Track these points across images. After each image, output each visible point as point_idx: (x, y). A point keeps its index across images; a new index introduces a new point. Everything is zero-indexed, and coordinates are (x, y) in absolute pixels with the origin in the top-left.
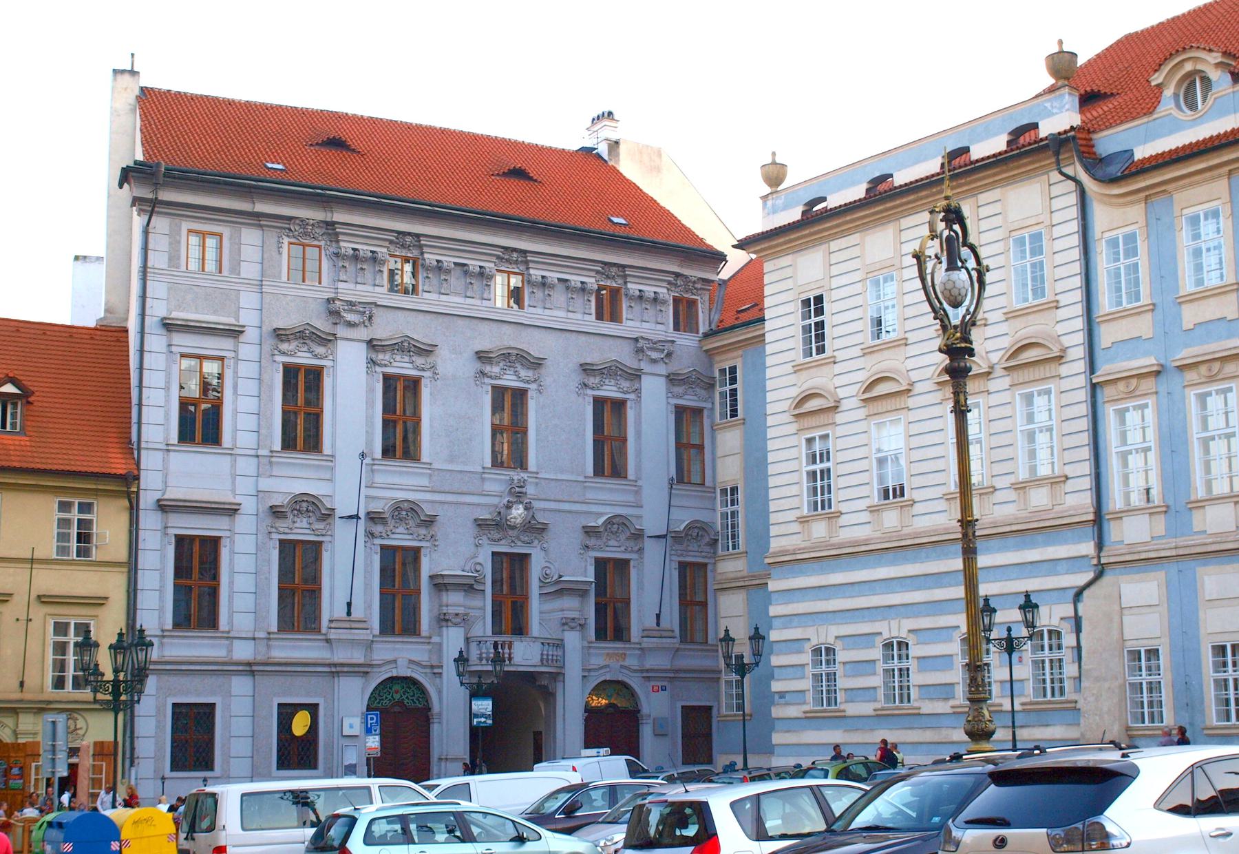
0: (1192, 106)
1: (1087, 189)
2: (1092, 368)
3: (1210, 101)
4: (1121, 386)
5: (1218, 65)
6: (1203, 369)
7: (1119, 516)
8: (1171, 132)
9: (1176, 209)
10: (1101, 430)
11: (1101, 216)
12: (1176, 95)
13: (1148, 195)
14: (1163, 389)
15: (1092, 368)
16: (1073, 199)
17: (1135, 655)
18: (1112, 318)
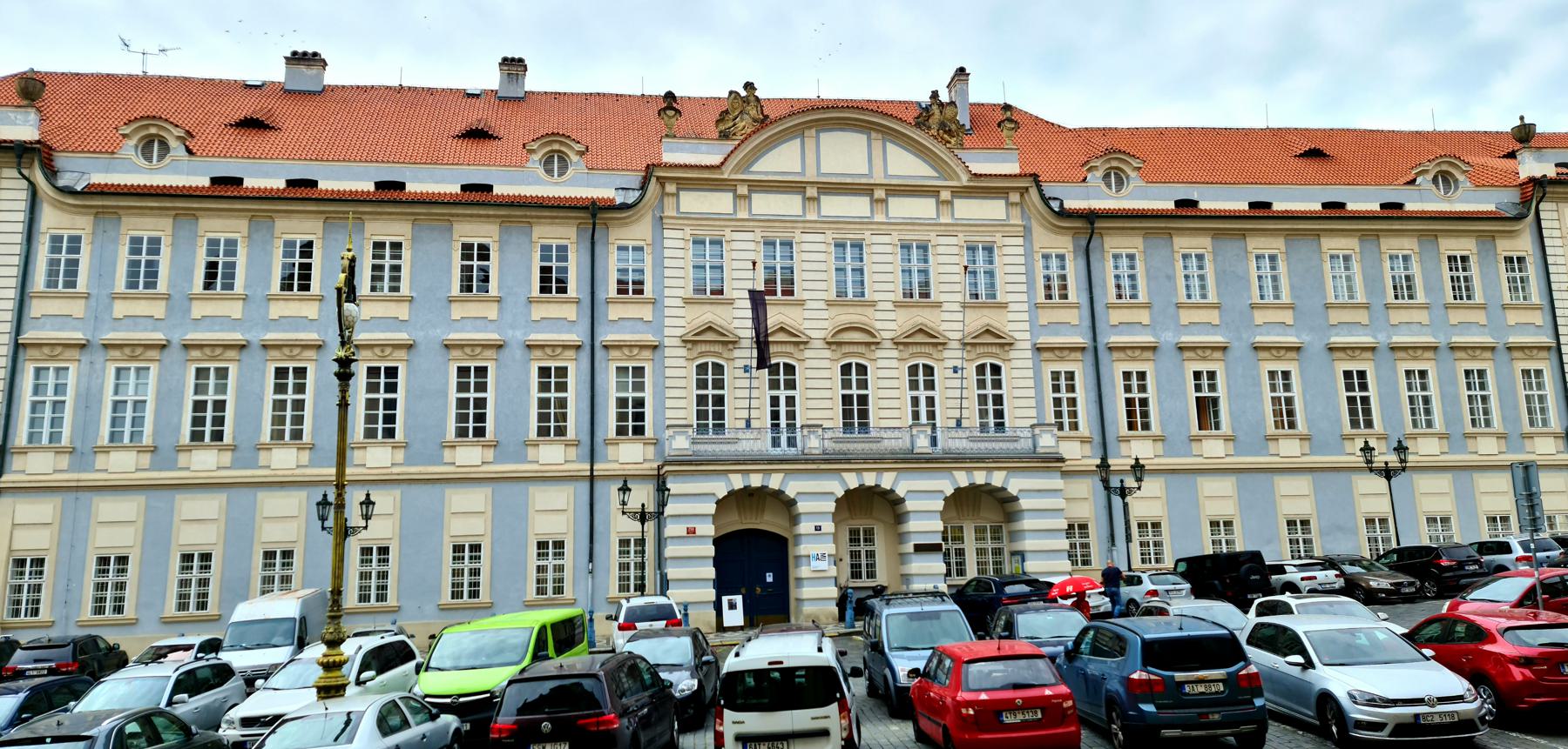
0: (149, 158)
1: (40, 193)
2: (18, 330)
3: (167, 160)
4: (46, 350)
5: (179, 138)
6: (127, 351)
7: (23, 451)
8: (128, 172)
9: (123, 230)
10: (17, 381)
11: (52, 220)
12: (136, 147)
13: (99, 213)
14: (83, 359)
15: (18, 330)
16: (24, 195)
17: (21, 563)
18: (42, 296)
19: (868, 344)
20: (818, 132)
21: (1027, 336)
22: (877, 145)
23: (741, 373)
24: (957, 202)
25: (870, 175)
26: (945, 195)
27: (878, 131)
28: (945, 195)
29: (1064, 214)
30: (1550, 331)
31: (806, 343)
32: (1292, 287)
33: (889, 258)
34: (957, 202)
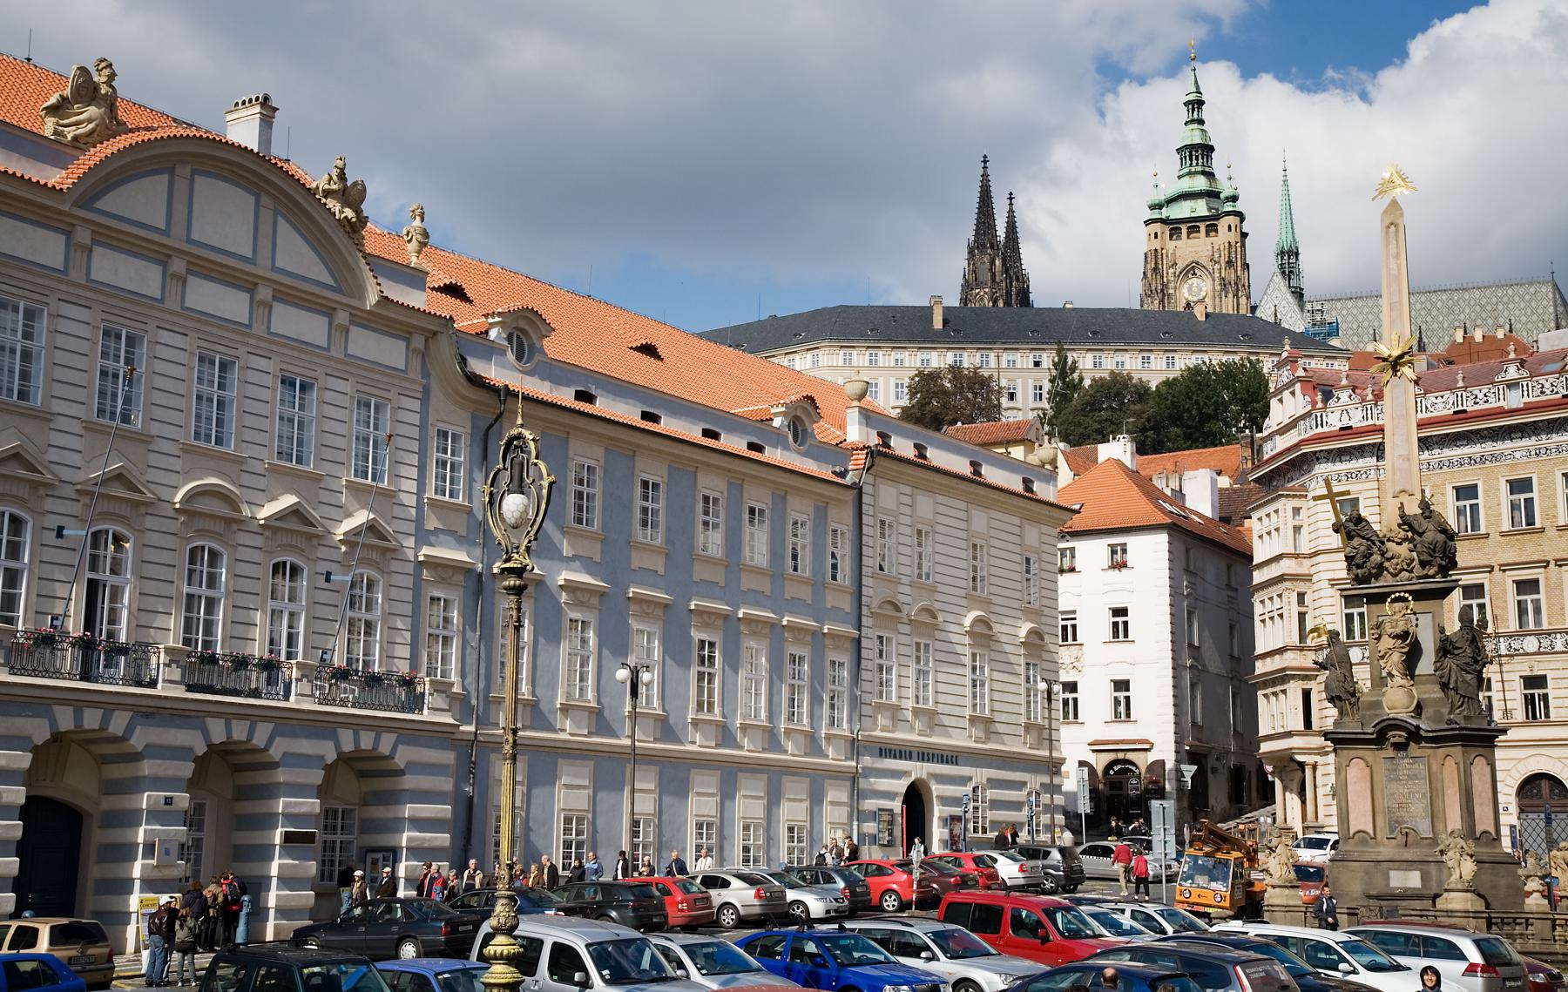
19: (229, 521)
20: (194, 172)
21: (410, 542)
22: (266, 216)
23: (50, 538)
24: (354, 330)
25: (166, 232)
26: (342, 317)
27: (268, 193)
28: (342, 317)
29: (475, 381)
30: (854, 621)
31: (147, 504)
32: (668, 529)
33: (84, 347)
34: (97, 250)
